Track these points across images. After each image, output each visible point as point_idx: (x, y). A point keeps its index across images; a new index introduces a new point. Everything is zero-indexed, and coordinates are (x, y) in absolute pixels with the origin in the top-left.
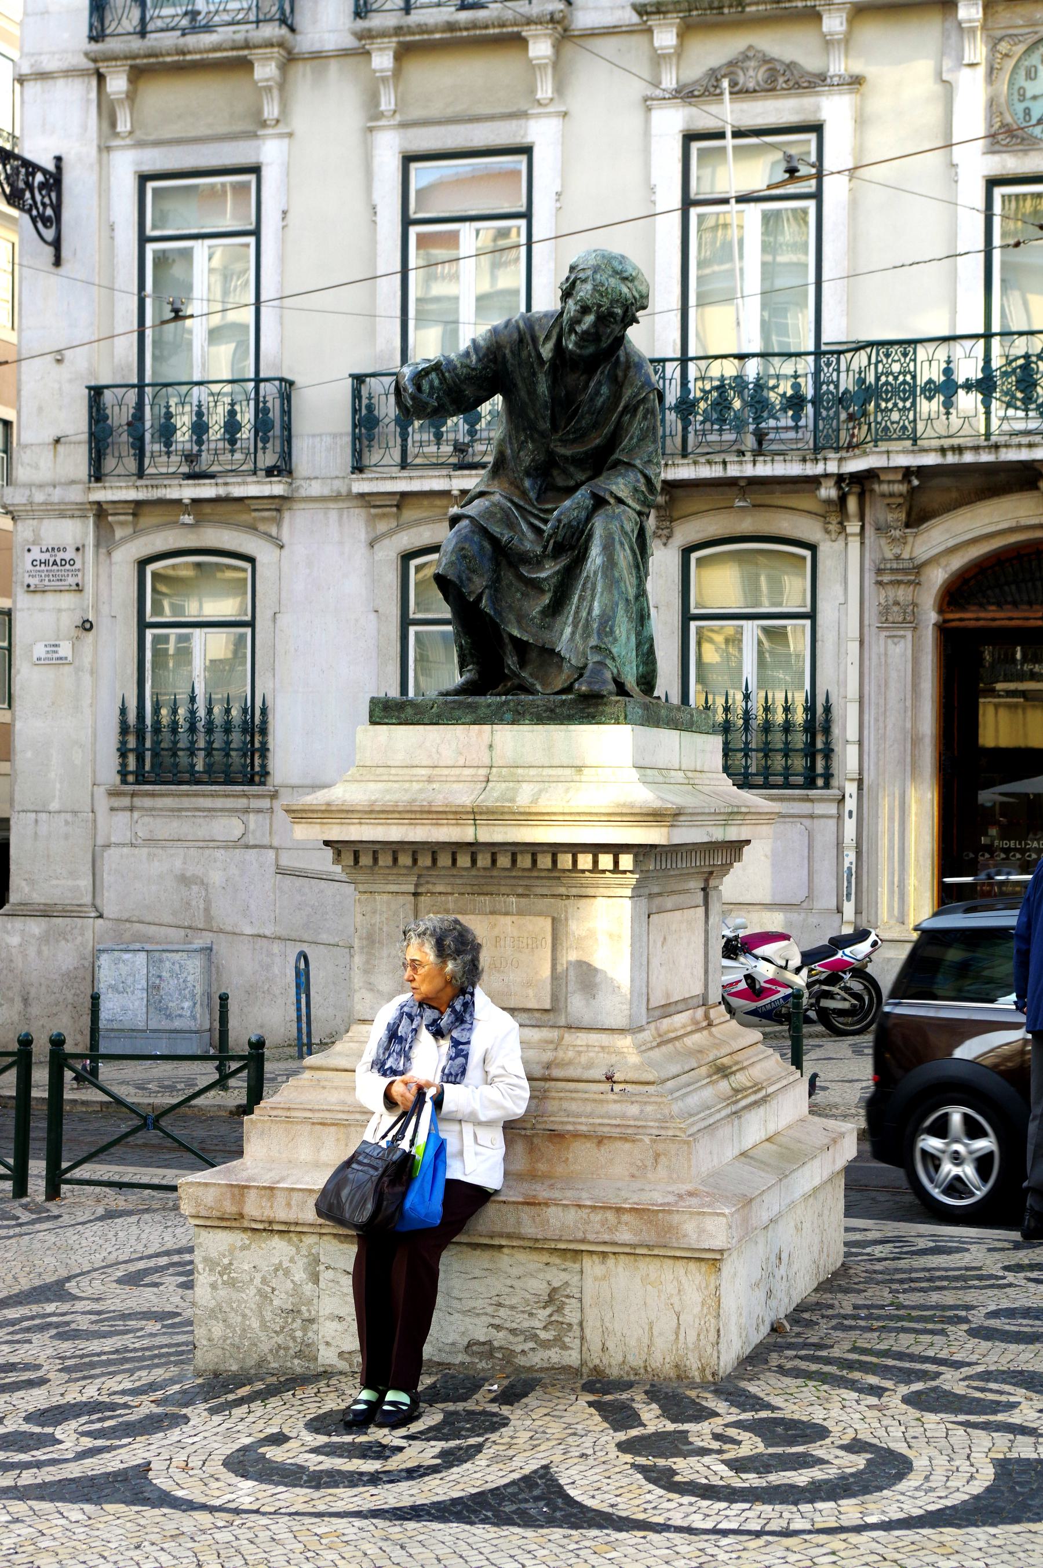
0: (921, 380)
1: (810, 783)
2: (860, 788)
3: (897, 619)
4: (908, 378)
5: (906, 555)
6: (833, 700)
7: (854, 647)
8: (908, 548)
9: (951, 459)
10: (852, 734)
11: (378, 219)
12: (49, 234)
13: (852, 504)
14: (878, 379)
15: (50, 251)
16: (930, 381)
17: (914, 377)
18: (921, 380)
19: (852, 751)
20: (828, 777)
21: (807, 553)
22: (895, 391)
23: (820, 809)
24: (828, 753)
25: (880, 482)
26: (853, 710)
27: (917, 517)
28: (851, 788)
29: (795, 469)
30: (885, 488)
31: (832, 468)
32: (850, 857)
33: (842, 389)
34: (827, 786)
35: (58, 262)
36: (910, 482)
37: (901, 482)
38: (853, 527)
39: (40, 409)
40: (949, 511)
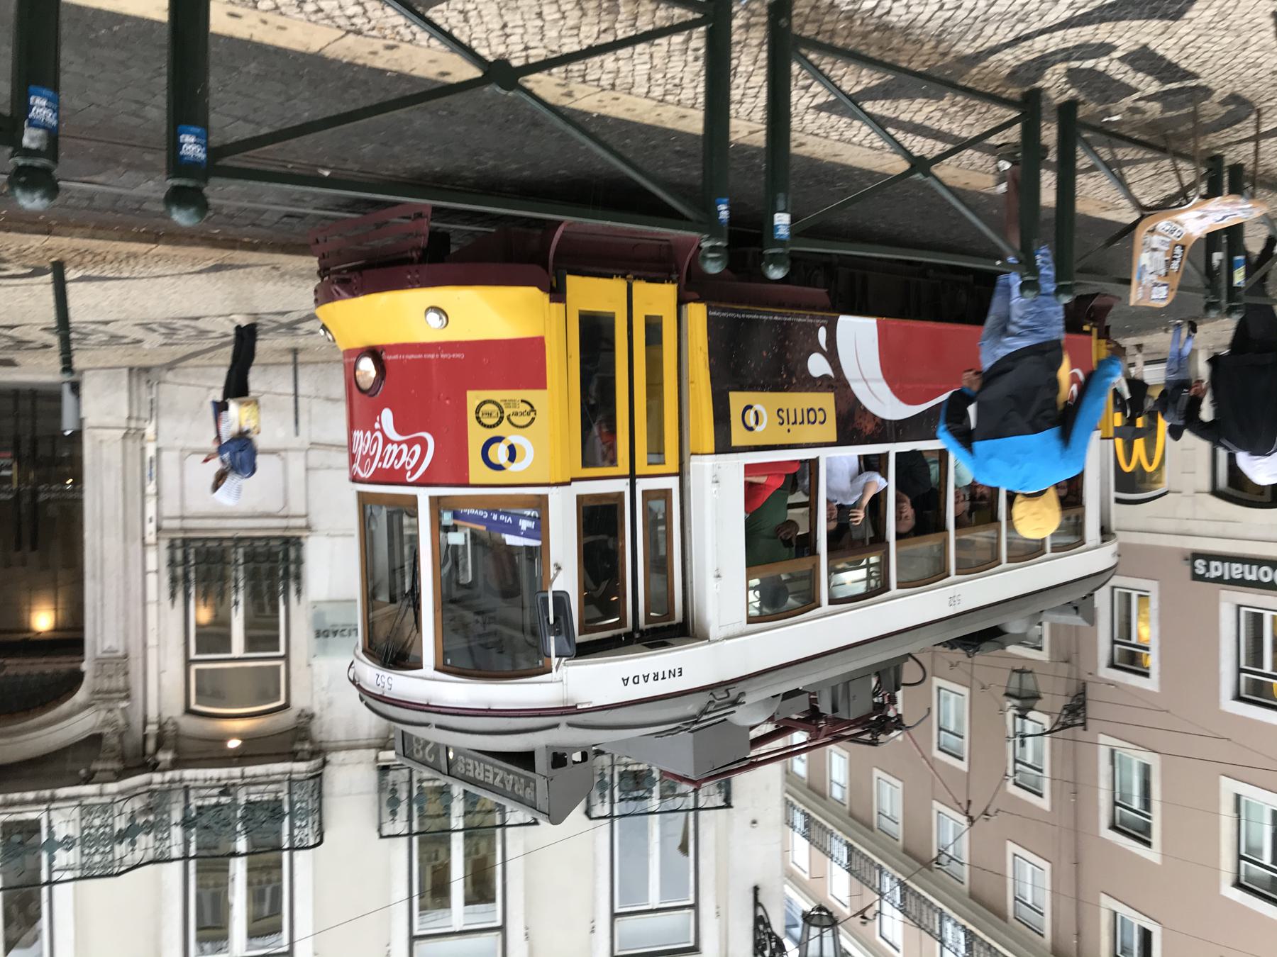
0: (77, 849)
1: (186, 542)
2: (143, 538)
3: (119, 663)
4: (87, 851)
5: (103, 714)
6: (169, 602)
7: (152, 641)
8: (101, 718)
9: (47, 793)
10: (152, 579)
11: (524, 931)
12: (760, 912)
13: (151, 745)
14: (112, 849)
15: (761, 899)
16: (68, 850)
17: (82, 852)
18: (77, 849)
19: (152, 563)
20: (172, 546)
21: (194, 706)
22: (97, 841)
23: (176, 524)
24: (172, 563)
25: (112, 770)
26: (152, 594)
27: (94, 741)
28: (151, 539)
29: (189, 774)
30: (109, 765)
31: (157, 777)
32: (151, 489)
33: (152, 835)
34: (172, 540)
35: (756, 889)
36: (88, 771)
37: (95, 772)
38: (152, 729)
39: (767, 788)
40: (56, 752)
